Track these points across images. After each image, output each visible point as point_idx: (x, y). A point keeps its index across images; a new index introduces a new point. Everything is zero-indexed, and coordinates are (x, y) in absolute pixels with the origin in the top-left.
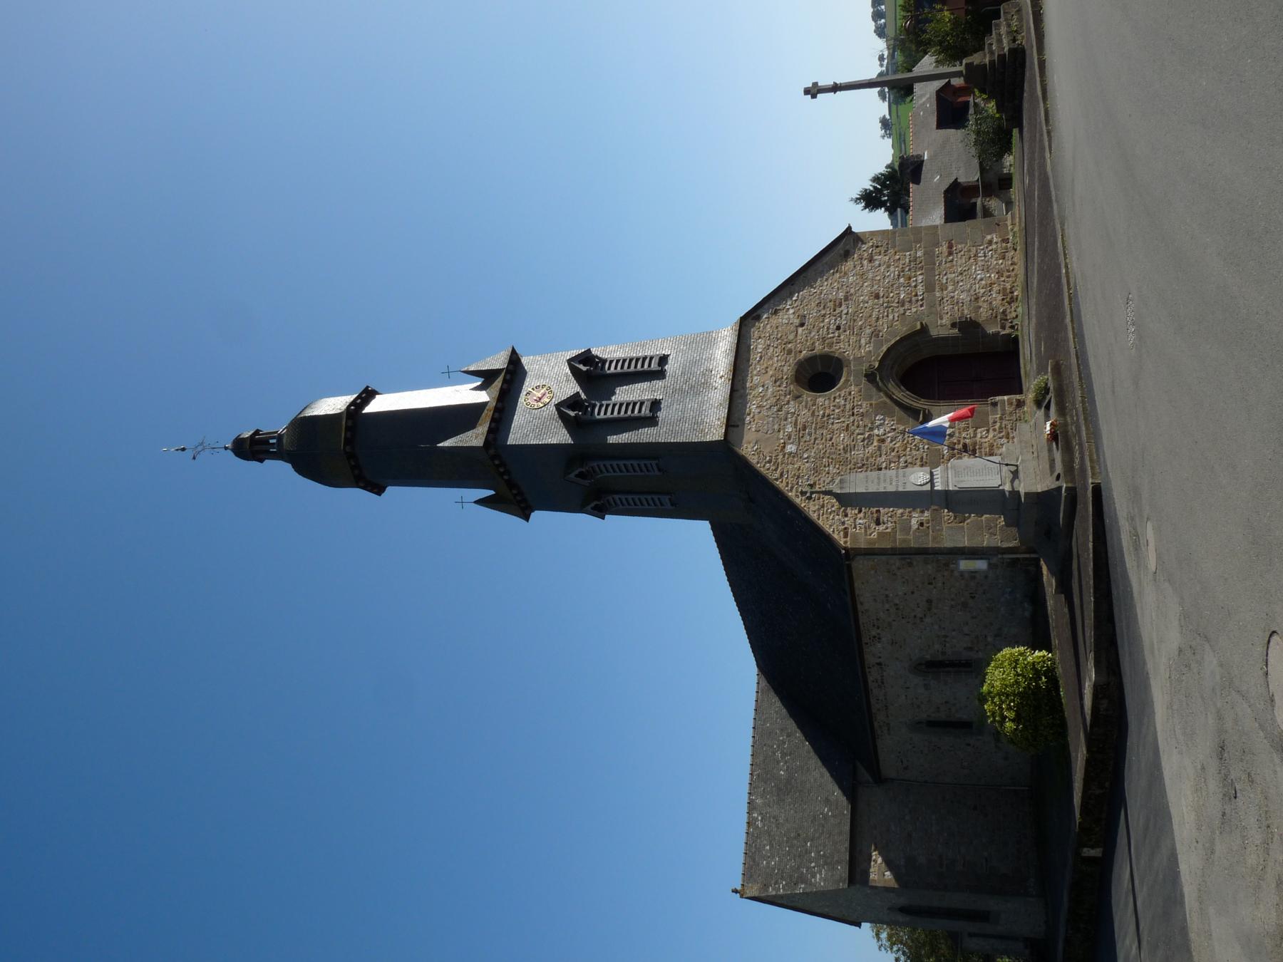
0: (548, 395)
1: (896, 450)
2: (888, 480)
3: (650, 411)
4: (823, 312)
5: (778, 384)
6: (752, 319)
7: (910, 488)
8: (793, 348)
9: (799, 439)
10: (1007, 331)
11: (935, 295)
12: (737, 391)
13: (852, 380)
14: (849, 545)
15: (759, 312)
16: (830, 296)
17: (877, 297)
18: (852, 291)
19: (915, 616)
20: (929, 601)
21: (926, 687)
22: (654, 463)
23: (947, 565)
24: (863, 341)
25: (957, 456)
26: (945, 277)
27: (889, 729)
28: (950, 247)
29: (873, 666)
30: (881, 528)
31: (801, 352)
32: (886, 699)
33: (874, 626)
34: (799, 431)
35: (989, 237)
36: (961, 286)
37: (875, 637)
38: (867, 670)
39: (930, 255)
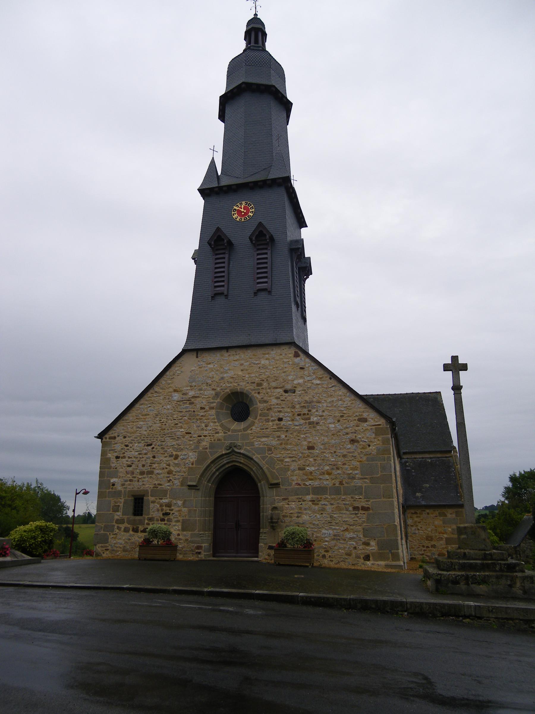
1: (167, 467)
4: (298, 406)
5: (231, 380)
6: (295, 352)
9: (182, 401)
11: (308, 494)
17: (311, 448)
24: (263, 439)
25: (160, 508)
26: (326, 503)
28: (364, 509)
30: (113, 460)
31: (259, 393)
34: (188, 400)
39: (358, 490)
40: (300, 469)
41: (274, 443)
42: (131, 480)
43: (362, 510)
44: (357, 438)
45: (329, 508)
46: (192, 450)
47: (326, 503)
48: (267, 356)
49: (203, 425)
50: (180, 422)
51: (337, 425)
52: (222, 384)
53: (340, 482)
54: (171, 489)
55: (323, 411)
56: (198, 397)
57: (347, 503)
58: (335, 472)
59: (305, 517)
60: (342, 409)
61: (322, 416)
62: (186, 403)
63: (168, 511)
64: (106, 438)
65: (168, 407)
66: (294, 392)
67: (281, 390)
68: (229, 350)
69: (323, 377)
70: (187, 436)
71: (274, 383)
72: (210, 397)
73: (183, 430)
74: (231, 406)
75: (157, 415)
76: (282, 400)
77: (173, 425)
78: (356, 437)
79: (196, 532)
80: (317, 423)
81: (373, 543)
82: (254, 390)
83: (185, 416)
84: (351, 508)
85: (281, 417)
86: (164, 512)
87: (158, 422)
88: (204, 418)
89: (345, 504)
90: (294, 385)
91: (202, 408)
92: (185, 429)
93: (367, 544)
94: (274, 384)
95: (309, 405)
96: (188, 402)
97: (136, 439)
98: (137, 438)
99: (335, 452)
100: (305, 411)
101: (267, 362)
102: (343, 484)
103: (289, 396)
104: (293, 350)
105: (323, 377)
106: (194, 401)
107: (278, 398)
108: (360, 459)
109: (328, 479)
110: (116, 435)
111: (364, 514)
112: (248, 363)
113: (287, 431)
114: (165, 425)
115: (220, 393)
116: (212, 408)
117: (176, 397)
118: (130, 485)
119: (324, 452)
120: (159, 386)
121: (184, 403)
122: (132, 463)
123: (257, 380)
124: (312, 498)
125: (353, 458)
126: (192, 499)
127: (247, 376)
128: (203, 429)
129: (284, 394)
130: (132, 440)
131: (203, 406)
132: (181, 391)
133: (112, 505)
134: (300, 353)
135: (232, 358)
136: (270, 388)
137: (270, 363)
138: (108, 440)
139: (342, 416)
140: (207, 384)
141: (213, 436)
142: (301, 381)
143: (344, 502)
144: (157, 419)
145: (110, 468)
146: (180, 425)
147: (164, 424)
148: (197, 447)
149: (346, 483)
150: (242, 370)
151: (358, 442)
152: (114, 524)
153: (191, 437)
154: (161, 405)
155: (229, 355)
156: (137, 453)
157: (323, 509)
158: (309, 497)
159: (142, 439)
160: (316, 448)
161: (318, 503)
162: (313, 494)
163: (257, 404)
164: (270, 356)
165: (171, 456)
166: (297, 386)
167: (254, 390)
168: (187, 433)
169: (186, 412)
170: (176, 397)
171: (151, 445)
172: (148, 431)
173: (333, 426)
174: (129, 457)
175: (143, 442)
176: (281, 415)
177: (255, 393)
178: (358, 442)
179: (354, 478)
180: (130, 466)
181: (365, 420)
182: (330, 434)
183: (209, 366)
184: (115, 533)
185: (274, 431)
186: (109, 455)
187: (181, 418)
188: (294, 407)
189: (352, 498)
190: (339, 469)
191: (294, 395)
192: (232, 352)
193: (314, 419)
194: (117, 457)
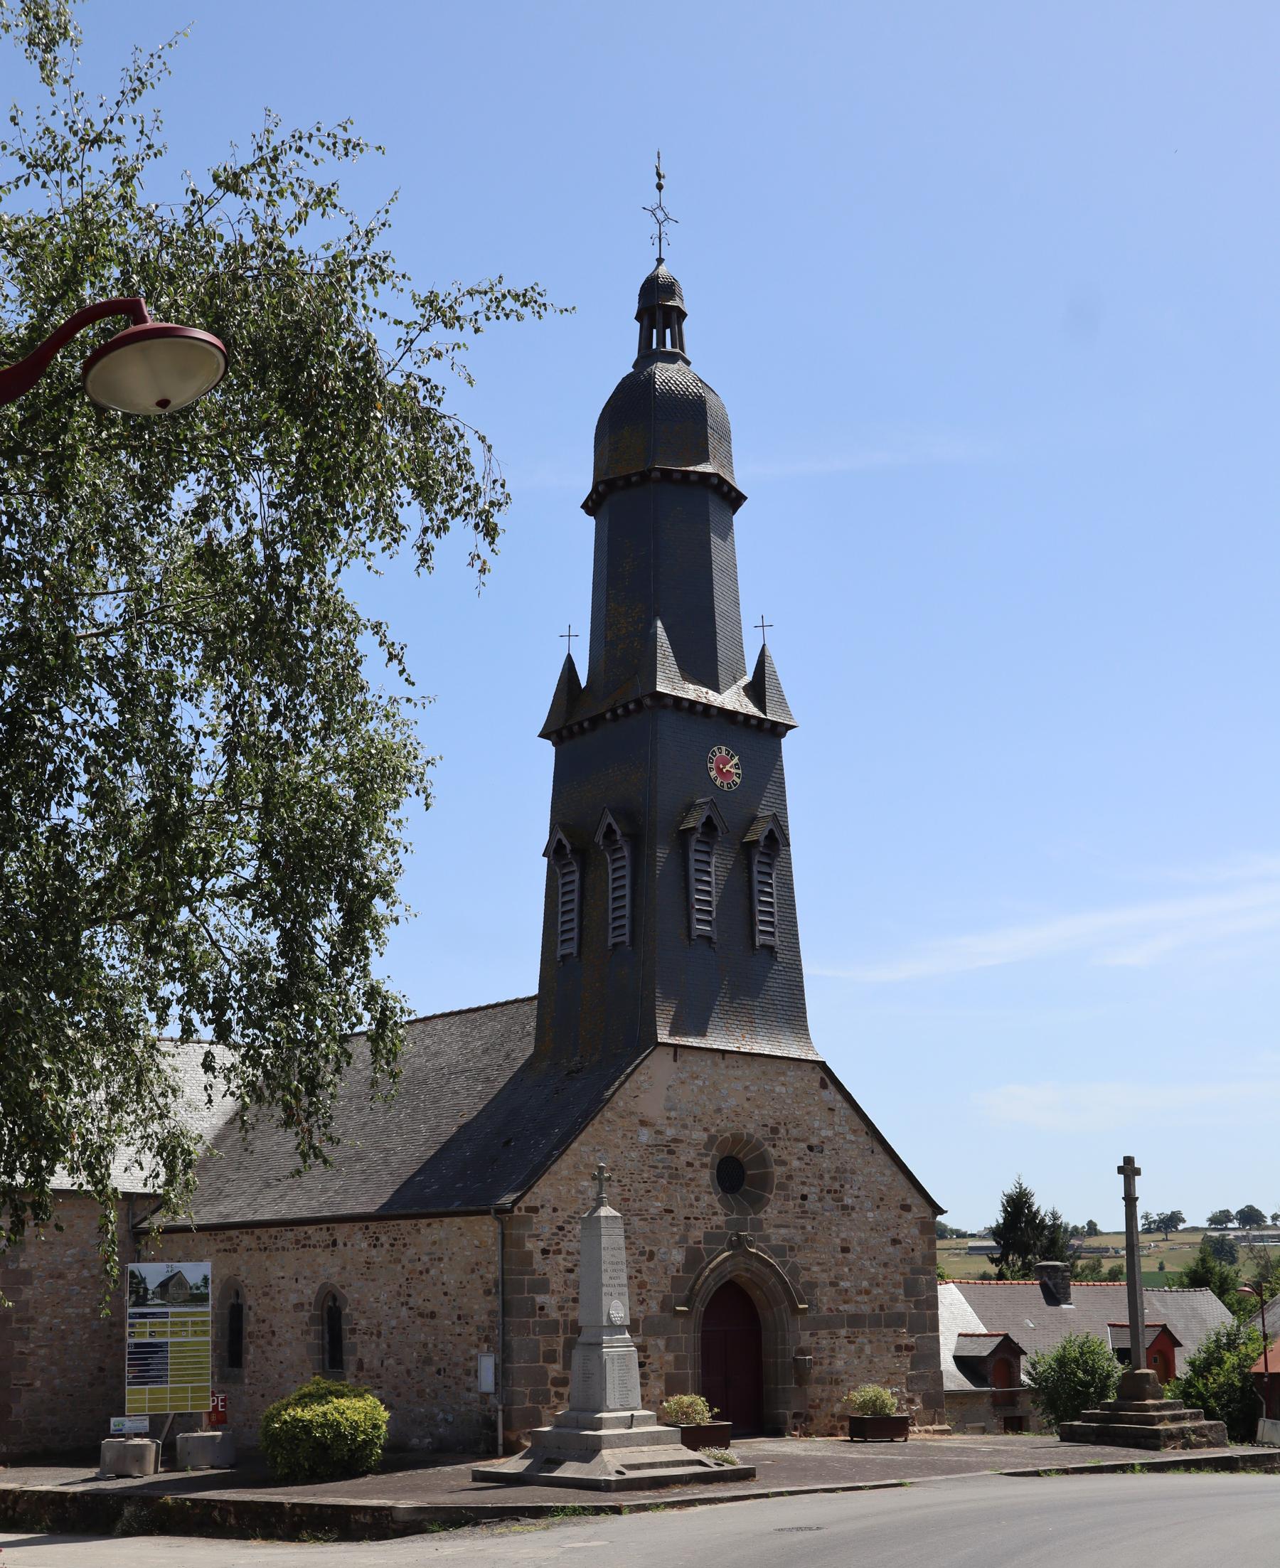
0: (725, 783)
1: (638, 1275)
2: (615, 1274)
4: (827, 1176)
7: (605, 1299)
8: (780, 1136)
10: (790, 1421)
12: (723, 1059)
14: (516, 1212)
15: (831, 1087)
16: (847, 1186)
17: (845, 1250)
18: (854, 1215)
19: (409, 1295)
20: (433, 1315)
21: (299, 1306)
22: (626, 938)
23: (487, 1339)
24: (783, 1231)
27: (225, 1250)
28: (909, 1348)
29: (331, 1235)
30: (538, 1257)
31: (774, 1146)
32: (277, 1249)
33: (395, 1239)
34: (666, 1146)
35: (918, 1400)
37: (377, 1239)
38: (324, 1226)
40: (833, 1284)
41: (799, 1238)
45: (868, 1350)
46: (676, 1243)
47: (866, 1341)
49: (692, 1197)
52: (718, 1121)
54: (646, 1318)
57: (890, 1339)
59: (839, 1364)
60: (883, 1188)
61: (858, 1197)
62: (663, 1151)
64: (520, 1209)
65: (633, 1155)
67: (804, 1145)
68: (727, 1056)
70: (668, 1217)
76: (806, 1164)
77: (642, 1192)
80: (853, 1208)
81: (918, 1400)
84: (893, 1349)
88: (693, 1184)
91: (689, 1164)
94: (794, 1132)
96: (666, 1149)
100: (836, 1186)
101: (783, 1090)
103: (815, 1156)
107: (799, 1159)
113: (814, 1219)
114: (629, 1190)
116: (704, 1165)
117: (645, 1136)
120: (612, 1109)
121: (658, 1151)
122: (575, 1265)
123: (771, 1122)
126: (680, 1335)
129: (808, 1152)
130: (569, 1216)
132: (652, 1125)
135: (731, 1072)
136: (789, 1139)
138: (523, 1213)
141: (709, 1219)
142: (830, 1133)
145: (533, 1273)
147: (626, 1188)
148: (684, 1239)
149: (888, 1308)
150: (748, 1099)
151: (900, 1242)
152: (549, 1386)
154: (619, 1151)
155: (727, 1067)
157: (861, 1350)
158: (843, 1332)
162: (849, 1326)
163: (772, 1167)
165: (642, 1253)
168: (666, 1211)
169: (663, 1168)
170: (645, 1136)
174: (569, 1253)
176: (805, 1190)
177: (769, 1145)
178: (900, 1242)
180: (571, 1271)
181: (906, 1208)
184: (552, 1404)
185: (798, 1218)
187: (654, 1179)
188: (821, 1177)
193: (848, 1201)
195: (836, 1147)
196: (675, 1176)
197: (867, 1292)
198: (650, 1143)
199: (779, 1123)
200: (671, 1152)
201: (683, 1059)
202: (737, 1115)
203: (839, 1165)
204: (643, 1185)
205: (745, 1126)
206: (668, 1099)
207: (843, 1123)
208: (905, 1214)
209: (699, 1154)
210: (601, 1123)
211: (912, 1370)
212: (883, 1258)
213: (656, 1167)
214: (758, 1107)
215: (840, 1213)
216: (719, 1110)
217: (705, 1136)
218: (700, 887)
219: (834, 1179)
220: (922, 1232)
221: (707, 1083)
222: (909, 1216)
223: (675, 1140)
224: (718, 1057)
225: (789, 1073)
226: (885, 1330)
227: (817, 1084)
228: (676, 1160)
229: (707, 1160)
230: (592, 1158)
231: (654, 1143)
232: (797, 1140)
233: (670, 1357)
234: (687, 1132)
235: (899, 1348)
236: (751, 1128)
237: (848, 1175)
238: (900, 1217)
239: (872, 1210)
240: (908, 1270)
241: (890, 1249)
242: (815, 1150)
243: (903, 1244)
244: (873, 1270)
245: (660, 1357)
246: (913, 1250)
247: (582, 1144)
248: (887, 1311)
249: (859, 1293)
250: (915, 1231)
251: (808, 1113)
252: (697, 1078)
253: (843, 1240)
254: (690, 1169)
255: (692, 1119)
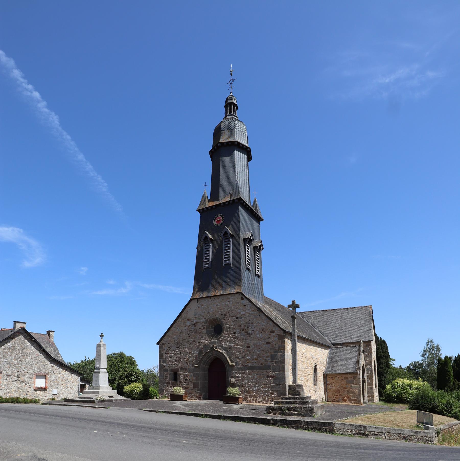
3: (205, 268)
4: (242, 326)
6: (242, 297)
12: (211, 299)
13: (212, 341)
17: (248, 347)
24: (227, 343)
28: (272, 377)
31: (225, 320)
34: (194, 325)
36: (250, 381)
42: (171, 364)
43: (271, 377)
44: (270, 341)
45: (256, 377)
48: (229, 300)
49: (201, 337)
50: (191, 336)
51: (260, 334)
52: (208, 316)
53: (261, 363)
54: (188, 368)
55: (254, 328)
56: (198, 323)
58: (259, 359)
60: (263, 326)
61: (254, 330)
63: (187, 379)
65: (186, 328)
66: (241, 319)
67: (235, 318)
68: (212, 298)
69: (254, 310)
70: (194, 342)
71: (231, 314)
72: (203, 323)
73: (192, 340)
74: (213, 326)
75: (181, 332)
76: (235, 323)
77: (188, 337)
78: (269, 340)
79: (199, 388)
80: (251, 334)
82: (223, 318)
83: (193, 333)
84: (266, 377)
85: (235, 331)
86: (186, 379)
87: (181, 336)
88: (201, 333)
89: (263, 375)
90: (241, 315)
91: (200, 328)
92: (192, 339)
93: (272, 394)
94: (232, 315)
95: (248, 324)
96: (194, 325)
97: (173, 345)
98: (173, 344)
99: (259, 349)
100: (246, 328)
101: (229, 303)
102: (263, 365)
103: (239, 320)
104: (241, 296)
105: (254, 310)
106: (196, 325)
107: (233, 322)
108: (271, 352)
109: (256, 362)
110: (164, 343)
111: (272, 379)
112: (220, 305)
115: (208, 320)
116: (204, 328)
117: (189, 323)
118: (171, 366)
119: (254, 349)
121: (192, 326)
123: (224, 313)
124: (248, 372)
125: (267, 351)
127: (220, 311)
128: (200, 339)
129: (236, 319)
130: (171, 345)
131: (200, 327)
132: (191, 320)
133: (165, 375)
134: (244, 297)
136: (230, 317)
137: (230, 303)
139: (263, 330)
140: (202, 316)
142: (244, 313)
143: (263, 374)
144: (181, 334)
146: (191, 337)
147: (184, 337)
149: (264, 364)
150: (217, 308)
151: (270, 343)
153: (196, 343)
155: (211, 301)
156: (173, 351)
159: (175, 344)
160: (251, 347)
161: (251, 374)
163: (224, 326)
164: (230, 300)
166: (242, 315)
167: (223, 318)
168: (194, 341)
169: (193, 330)
170: (189, 323)
171: (179, 347)
172: (177, 340)
173: (259, 335)
174: (171, 354)
175: (176, 346)
176: (235, 331)
177: (223, 320)
178: (270, 343)
179: (267, 361)
181: (273, 332)
182: (257, 340)
183: (203, 307)
186: (162, 352)
187: (191, 333)
188: (241, 326)
189: (267, 371)
190: (261, 357)
191: (241, 320)
192: (213, 298)
193: (250, 332)
194: (166, 353)
195: (246, 316)
196: (196, 332)
197: (256, 359)
198: (190, 324)
199: (227, 313)
200: (195, 326)
201: (200, 301)
202: (214, 313)
203: (247, 322)
204: (188, 335)
205: (216, 316)
206: (195, 312)
207: (249, 309)
208: (272, 334)
209: (203, 325)
210: (179, 322)
211: (273, 384)
212: (263, 348)
213: (191, 330)
214: (220, 310)
215: (247, 336)
216: (208, 313)
217: (205, 320)
218: (206, 255)
219: (245, 326)
220: (278, 339)
221: (206, 306)
222: (274, 334)
223: (196, 323)
224: (209, 299)
225: (231, 298)
226: (263, 371)
227: (240, 299)
228: (196, 328)
229: (205, 326)
230: (176, 330)
231: (191, 324)
232: (232, 317)
233: (195, 378)
234: (200, 320)
235: (268, 377)
236: (218, 316)
237: (250, 324)
238: (270, 335)
239: (259, 334)
240: (273, 351)
241: (266, 345)
242: (239, 318)
243: (271, 344)
244: (258, 352)
245: (192, 378)
246: (275, 345)
247: (174, 327)
248: (264, 365)
249: (253, 360)
250: (277, 339)
251: (236, 308)
252: (203, 305)
253: (248, 344)
254: (200, 330)
255: (201, 316)
